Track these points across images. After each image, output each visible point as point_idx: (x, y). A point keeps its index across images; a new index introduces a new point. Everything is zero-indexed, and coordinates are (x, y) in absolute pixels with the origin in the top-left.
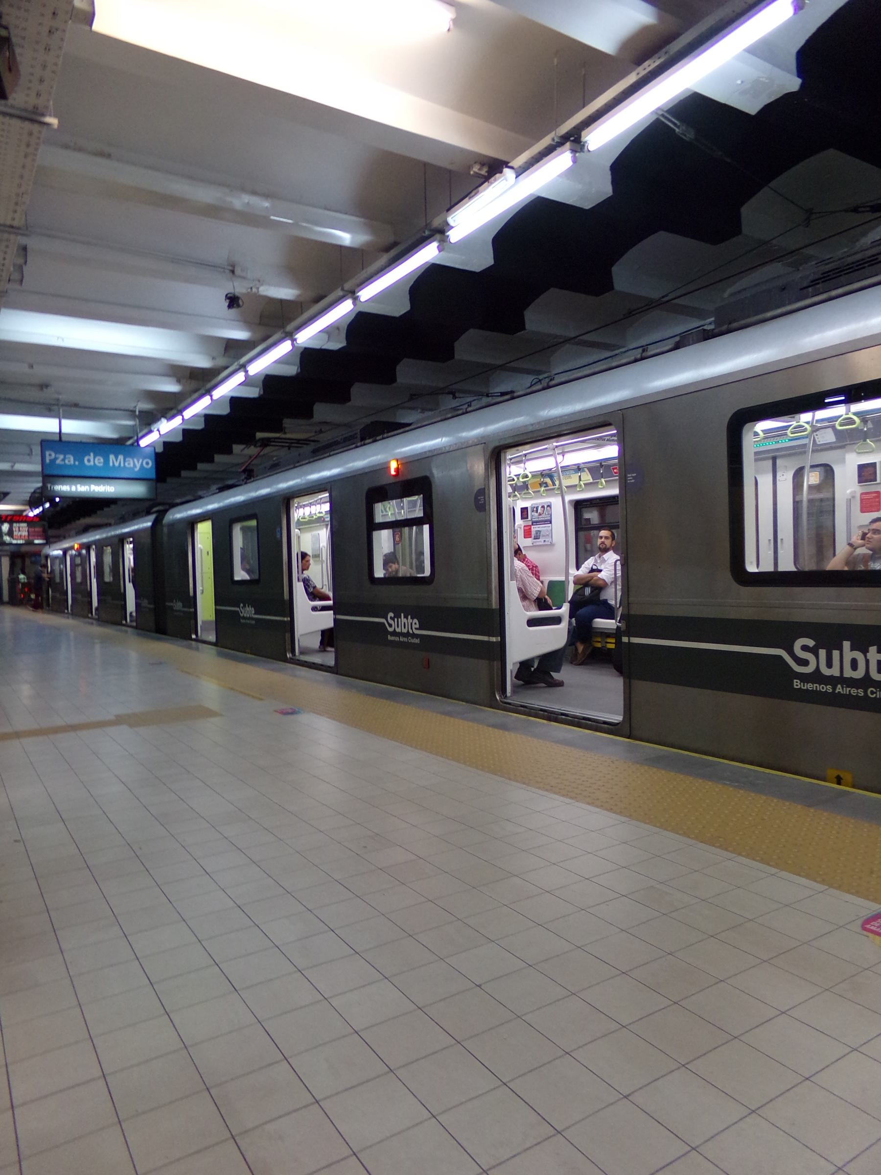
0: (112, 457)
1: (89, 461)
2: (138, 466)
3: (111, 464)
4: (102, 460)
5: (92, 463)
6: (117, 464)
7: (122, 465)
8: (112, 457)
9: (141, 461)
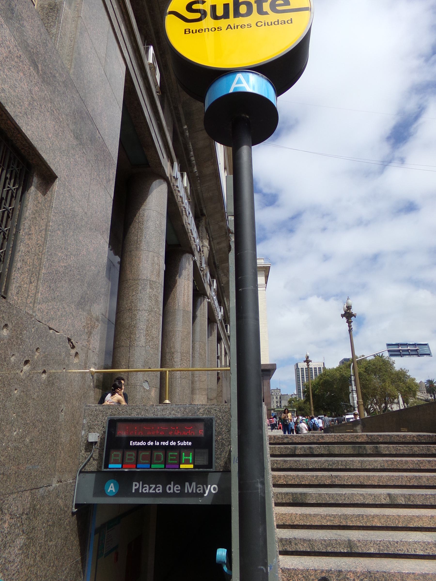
0: (187, 484)
1: (170, 489)
2: (207, 492)
3: (186, 491)
4: (179, 488)
5: (172, 491)
6: (190, 491)
7: (194, 492)
8: (187, 484)
9: (209, 486)
